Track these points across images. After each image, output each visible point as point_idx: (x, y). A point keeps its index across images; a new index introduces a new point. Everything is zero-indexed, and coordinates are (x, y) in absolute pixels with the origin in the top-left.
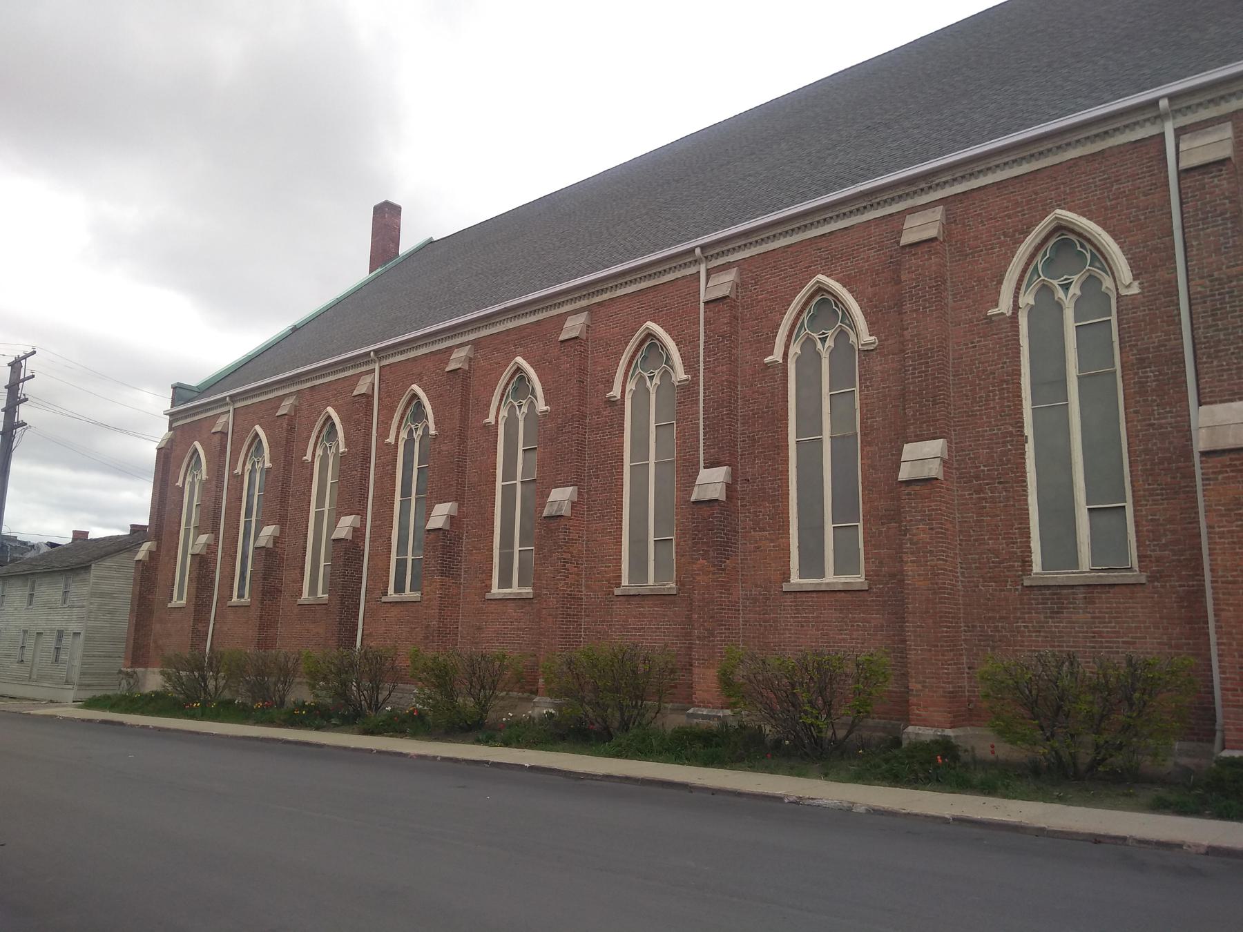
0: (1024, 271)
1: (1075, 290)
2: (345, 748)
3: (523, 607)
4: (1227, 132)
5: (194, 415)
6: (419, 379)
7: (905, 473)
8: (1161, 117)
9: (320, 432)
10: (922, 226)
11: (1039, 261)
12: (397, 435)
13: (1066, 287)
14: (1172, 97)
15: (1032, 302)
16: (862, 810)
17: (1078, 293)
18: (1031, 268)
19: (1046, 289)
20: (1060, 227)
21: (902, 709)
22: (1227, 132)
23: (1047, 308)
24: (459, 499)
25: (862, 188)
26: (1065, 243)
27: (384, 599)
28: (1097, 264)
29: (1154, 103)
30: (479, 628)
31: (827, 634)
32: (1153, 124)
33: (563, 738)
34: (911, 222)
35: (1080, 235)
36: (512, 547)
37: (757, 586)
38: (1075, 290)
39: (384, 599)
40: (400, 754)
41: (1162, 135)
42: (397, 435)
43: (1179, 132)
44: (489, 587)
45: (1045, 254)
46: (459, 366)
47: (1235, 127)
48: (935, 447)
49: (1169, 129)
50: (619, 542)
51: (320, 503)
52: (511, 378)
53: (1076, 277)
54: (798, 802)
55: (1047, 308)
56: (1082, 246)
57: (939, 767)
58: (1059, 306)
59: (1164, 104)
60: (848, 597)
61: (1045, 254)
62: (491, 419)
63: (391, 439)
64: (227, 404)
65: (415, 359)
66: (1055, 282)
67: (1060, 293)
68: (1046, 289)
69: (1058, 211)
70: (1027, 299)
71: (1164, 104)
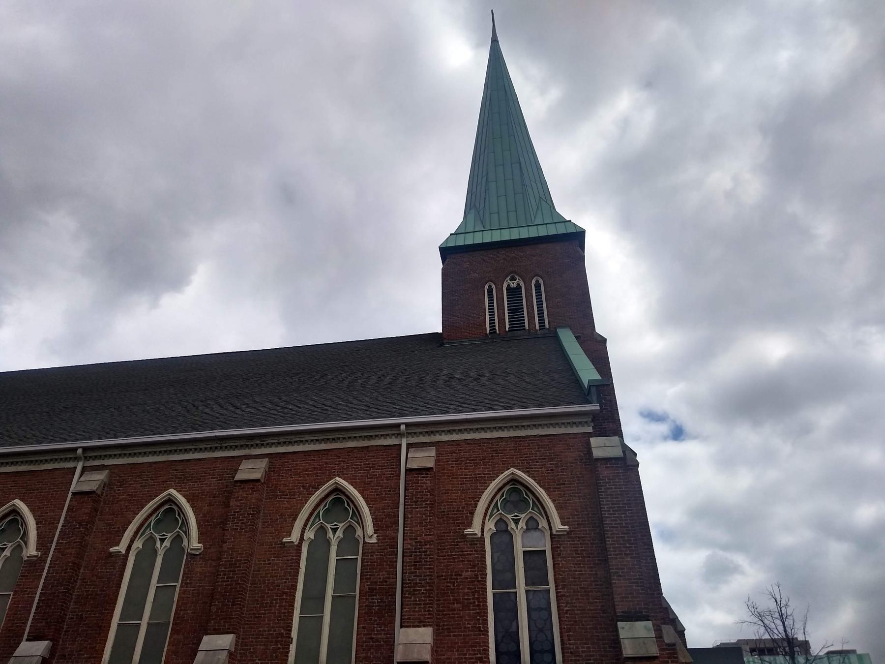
0: (311, 514)
1: (339, 533)
4: (432, 452)
8: (400, 435)
10: (252, 470)
11: (321, 510)
13: (335, 530)
14: (408, 425)
17: (341, 536)
18: (316, 513)
19: (322, 529)
20: (338, 490)
22: (432, 452)
23: (321, 543)
26: (338, 501)
34: (246, 465)
35: (348, 497)
38: (339, 533)
43: (409, 446)
47: (437, 451)
49: (404, 443)
55: (321, 543)
56: (348, 505)
59: (403, 427)
66: (329, 526)
67: (330, 534)
68: (322, 529)
69: (337, 478)
70: (310, 535)
71: (403, 427)
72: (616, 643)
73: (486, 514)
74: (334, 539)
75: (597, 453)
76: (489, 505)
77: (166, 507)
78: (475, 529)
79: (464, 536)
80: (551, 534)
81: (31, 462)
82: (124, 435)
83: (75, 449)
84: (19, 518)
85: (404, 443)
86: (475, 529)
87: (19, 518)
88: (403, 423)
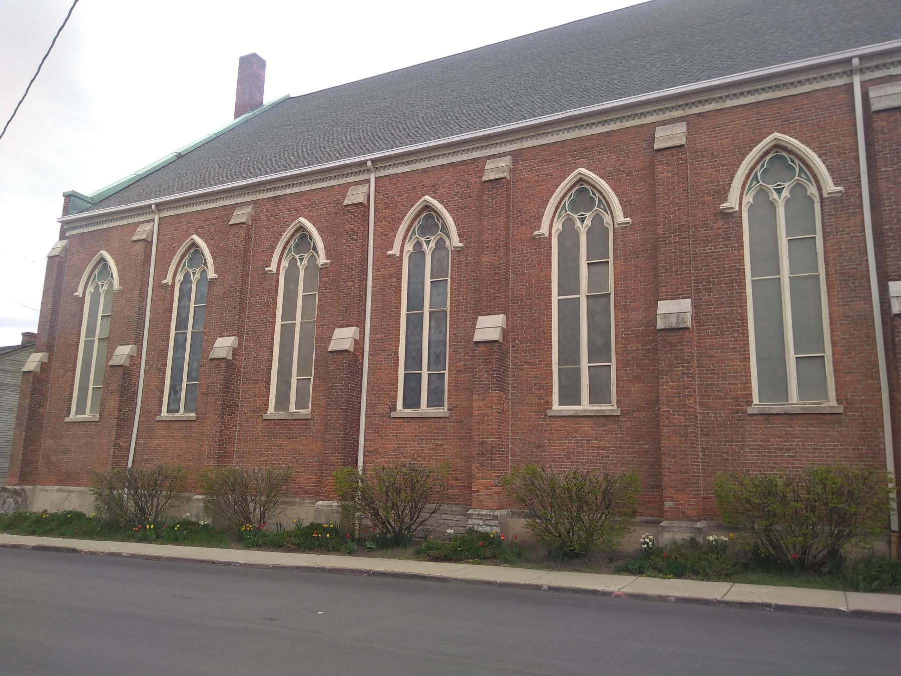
1: (786, 193)
3: (604, 425)
5: (643, 115)
6: (433, 191)
7: (660, 325)
9: (287, 243)
10: (671, 135)
11: (759, 171)
12: (401, 246)
13: (779, 191)
14: (862, 58)
15: (752, 201)
17: (789, 196)
18: (753, 174)
24: (239, 334)
27: (393, 414)
28: (803, 175)
29: (849, 61)
30: (539, 446)
36: (577, 360)
38: (786, 193)
39: (393, 414)
41: (851, 86)
42: (401, 246)
44: (549, 404)
45: (763, 166)
46: (505, 175)
48: (685, 305)
49: (857, 81)
50: (747, 359)
51: (289, 312)
52: (570, 190)
53: (786, 185)
56: (792, 161)
58: (773, 205)
61: (763, 166)
62: (544, 230)
63: (395, 251)
64: (368, 171)
65: (425, 171)
67: (775, 195)
68: (762, 193)
70: (748, 199)
71: (856, 61)
82: (476, 128)
83: (365, 162)
88: (855, 56)
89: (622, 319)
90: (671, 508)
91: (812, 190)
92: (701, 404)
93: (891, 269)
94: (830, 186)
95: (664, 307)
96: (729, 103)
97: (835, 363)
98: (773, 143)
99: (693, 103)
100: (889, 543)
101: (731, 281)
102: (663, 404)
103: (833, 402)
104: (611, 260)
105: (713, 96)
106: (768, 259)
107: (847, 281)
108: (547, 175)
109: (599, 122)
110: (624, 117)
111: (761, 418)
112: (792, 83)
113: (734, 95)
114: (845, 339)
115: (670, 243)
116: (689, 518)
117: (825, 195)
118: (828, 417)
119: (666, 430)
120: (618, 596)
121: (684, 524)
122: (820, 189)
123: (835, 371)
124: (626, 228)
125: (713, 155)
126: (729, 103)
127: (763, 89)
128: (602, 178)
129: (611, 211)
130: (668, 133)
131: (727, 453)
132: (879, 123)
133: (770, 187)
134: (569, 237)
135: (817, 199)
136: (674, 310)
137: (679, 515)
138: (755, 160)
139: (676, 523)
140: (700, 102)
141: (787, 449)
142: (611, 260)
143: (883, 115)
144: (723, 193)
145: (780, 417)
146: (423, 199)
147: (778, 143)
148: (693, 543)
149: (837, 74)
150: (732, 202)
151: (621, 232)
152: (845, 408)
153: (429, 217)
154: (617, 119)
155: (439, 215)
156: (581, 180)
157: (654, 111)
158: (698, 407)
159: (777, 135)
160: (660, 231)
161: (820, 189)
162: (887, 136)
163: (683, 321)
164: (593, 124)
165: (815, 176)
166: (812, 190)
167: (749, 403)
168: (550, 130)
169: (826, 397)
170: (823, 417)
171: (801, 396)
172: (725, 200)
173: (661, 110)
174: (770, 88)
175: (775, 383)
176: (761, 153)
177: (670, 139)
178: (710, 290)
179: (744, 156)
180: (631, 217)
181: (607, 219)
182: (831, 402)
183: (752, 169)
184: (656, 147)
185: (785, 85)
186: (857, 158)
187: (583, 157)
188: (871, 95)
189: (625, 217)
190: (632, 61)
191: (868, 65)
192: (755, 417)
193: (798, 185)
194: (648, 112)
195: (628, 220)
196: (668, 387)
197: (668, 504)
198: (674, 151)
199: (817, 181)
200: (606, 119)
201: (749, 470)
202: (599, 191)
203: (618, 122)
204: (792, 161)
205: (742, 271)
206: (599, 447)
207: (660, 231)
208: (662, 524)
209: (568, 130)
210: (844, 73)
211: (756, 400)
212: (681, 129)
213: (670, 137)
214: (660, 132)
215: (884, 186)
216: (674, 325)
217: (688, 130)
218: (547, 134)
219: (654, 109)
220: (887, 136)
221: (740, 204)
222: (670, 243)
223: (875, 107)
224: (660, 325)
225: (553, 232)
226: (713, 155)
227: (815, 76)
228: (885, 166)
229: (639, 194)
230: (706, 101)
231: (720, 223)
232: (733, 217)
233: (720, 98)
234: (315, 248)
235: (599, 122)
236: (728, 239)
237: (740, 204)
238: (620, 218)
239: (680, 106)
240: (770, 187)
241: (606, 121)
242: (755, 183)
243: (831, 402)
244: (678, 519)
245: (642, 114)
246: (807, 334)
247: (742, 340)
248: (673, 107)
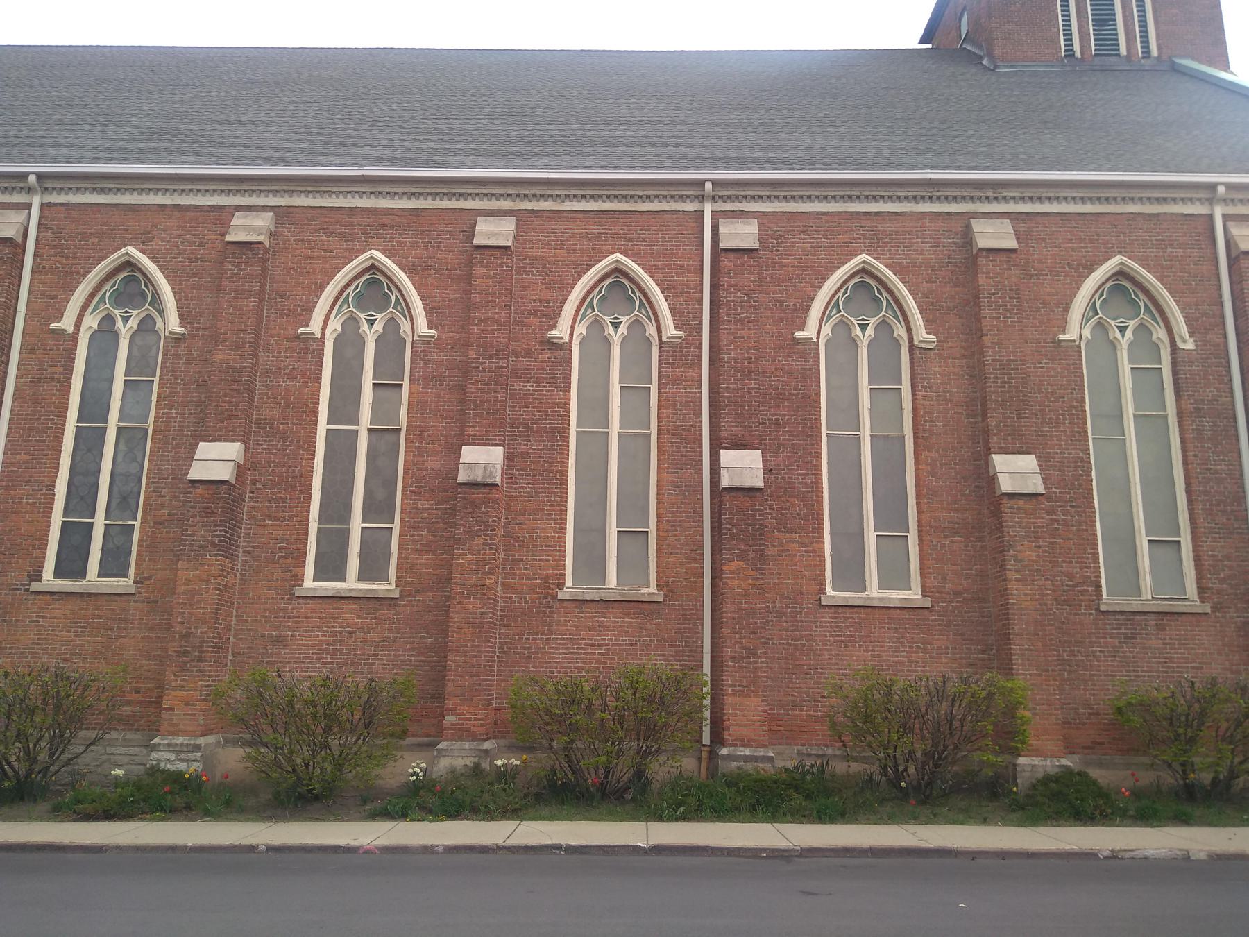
0: (584, 299)
1: (623, 329)
2: (173, 849)
3: (376, 610)
8: (702, 199)
10: (495, 231)
12: (78, 317)
13: (616, 326)
14: (715, 183)
16: (263, 848)
20: (618, 271)
21: (1010, 738)
22: (752, 227)
23: (597, 341)
25: (366, 173)
27: (35, 587)
29: (701, 183)
30: (277, 640)
31: (879, 656)
32: (1202, 204)
33: (538, 798)
35: (631, 280)
36: (346, 518)
37: (782, 597)
38: (623, 329)
39: (35, 587)
40: (335, 849)
41: (701, 214)
42: (78, 317)
44: (299, 579)
46: (261, 238)
47: (760, 225)
49: (708, 208)
52: (356, 277)
53: (624, 319)
54: (1114, 856)
55: (597, 341)
56: (633, 292)
57: (1067, 800)
58: (607, 341)
59: (708, 186)
60: (906, 615)
62: (315, 327)
63: (66, 324)
64: (30, 190)
65: (132, 208)
67: (611, 330)
68: (597, 324)
70: (581, 329)
71: (708, 186)
72: (992, 480)
73: (823, 314)
74: (616, 338)
75: (982, 242)
76: (828, 304)
77: (367, 277)
78: (809, 332)
79: (796, 342)
80: (912, 347)
81: (102, 191)
84: (139, 275)
85: (708, 208)
86: (809, 332)
87: (139, 275)
89: (414, 465)
90: (453, 724)
91: (651, 330)
92: (504, 585)
93: (724, 435)
94: (670, 330)
95: (470, 454)
96: (568, 206)
97: (659, 540)
98: (613, 266)
99: (526, 196)
100: (699, 759)
101: (553, 430)
102: (456, 583)
103: (653, 589)
104: (406, 383)
105: (550, 192)
106: (596, 407)
107: (679, 444)
108: (326, 251)
109: (404, 193)
110: (438, 194)
111: (572, 605)
112: (640, 197)
113: (575, 196)
114: (671, 512)
115: (484, 372)
116: (474, 737)
117: (664, 339)
118: (647, 606)
119: (456, 618)
120: (367, 852)
121: (467, 745)
122: (659, 331)
123: (658, 550)
124: (429, 342)
125: (544, 267)
126: (568, 206)
127: (608, 196)
128: (403, 270)
129: (411, 316)
130: (492, 227)
131: (530, 649)
132: (726, 264)
133: (606, 318)
134: (349, 342)
135: (655, 342)
136: (481, 459)
137: (464, 733)
138: (592, 283)
139: (457, 745)
140: (534, 195)
141: (599, 645)
142: (406, 383)
143: (732, 255)
144: (551, 319)
145: (595, 604)
146: (123, 251)
147: (619, 266)
148: (476, 770)
149: (688, 197)
150: (561, 331)
151: (423, 348)
152: (666, 596)
153: (130, 280)
154: (428, 194)
155: (149, 280)
156: (373, 267)
157: (477, 195)
158: (499, 588)
159: (618, 256)
160: (472, 354)
161: (659, 331)
162: (733, 281)
163: (492, 476)
164: (396, 193)
165: (655, 314)
166: (651, 330)
167: (561, 586)
168: (335, 189)
169: (647, 584)
170: (640, 605)
171: (619, 582)
172: (554, 326)
173: (485, 195)
174: (616, 197)
175: (592, 563)
176: (599, 275)
177: (494, 235)
178: (527, 439)
179: (580, 274)
180: (437, 329)
181: (405, 326)
182: (651, 589)
183: (588, 293)
184: (476, 242)
185: (632, 197)
186: (701, 300)
187: (379, 236)
188: (721, 229)
189: (429, 328)
190: (456, 123)
191: (721, 193)
192: (565, 604)
193: (637, 322)
194: (470, 194)
195: (432, 332)
196: (464, 560)
197: (450, 719)
198: (497, 252)
199: (657, 321)
200: (413, 190)
201: (552, 672)
202: (397, 287)
203: (430, 198)
204: (633, 292)
205: (566, 419)
206: (365, 642)
207: (472, 354)
208: (440, 747)
209: (361, 194)
210: (696, 197)
211: (569, 582)
212: (509, 224)
213: (494, 234)
214: (482, 224)
215: (725, 337)
216: (479, 480)
217: (517, 229)
218: (330, 193)
219: (477, 191)
220: (733, 281)
221: (571, 334)
222: (484, 372)
223: (723, 245)
224: (462, 477)
225: (328, 332)
226: (544, 267)
227: (665, 193)
228: (728, 315)
229: (451, 300)
230: (542, 196)
231: (546, 355)
232: (560, 349)
233: (559, 196)
234: (157, 301)
235: (404, 193)
236: (553, 375)
237: (571, 334)
238: (423, 328)
239: (509, 195)
240: (606, 318)
241: (413, 194)
242: (590, 311)
243: (651, 589)
244: (461, 739)
245: (461, 195)
246: (632, 503)
247: (559, 506)
248: (501, 195)
